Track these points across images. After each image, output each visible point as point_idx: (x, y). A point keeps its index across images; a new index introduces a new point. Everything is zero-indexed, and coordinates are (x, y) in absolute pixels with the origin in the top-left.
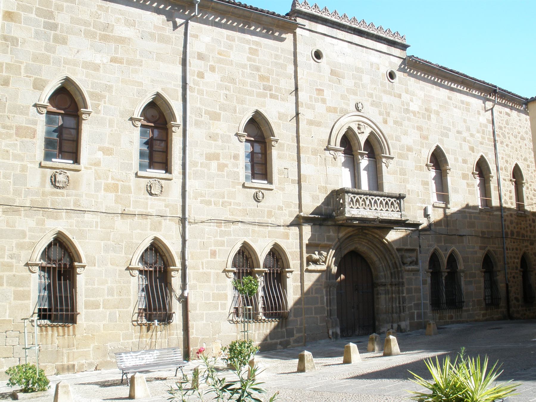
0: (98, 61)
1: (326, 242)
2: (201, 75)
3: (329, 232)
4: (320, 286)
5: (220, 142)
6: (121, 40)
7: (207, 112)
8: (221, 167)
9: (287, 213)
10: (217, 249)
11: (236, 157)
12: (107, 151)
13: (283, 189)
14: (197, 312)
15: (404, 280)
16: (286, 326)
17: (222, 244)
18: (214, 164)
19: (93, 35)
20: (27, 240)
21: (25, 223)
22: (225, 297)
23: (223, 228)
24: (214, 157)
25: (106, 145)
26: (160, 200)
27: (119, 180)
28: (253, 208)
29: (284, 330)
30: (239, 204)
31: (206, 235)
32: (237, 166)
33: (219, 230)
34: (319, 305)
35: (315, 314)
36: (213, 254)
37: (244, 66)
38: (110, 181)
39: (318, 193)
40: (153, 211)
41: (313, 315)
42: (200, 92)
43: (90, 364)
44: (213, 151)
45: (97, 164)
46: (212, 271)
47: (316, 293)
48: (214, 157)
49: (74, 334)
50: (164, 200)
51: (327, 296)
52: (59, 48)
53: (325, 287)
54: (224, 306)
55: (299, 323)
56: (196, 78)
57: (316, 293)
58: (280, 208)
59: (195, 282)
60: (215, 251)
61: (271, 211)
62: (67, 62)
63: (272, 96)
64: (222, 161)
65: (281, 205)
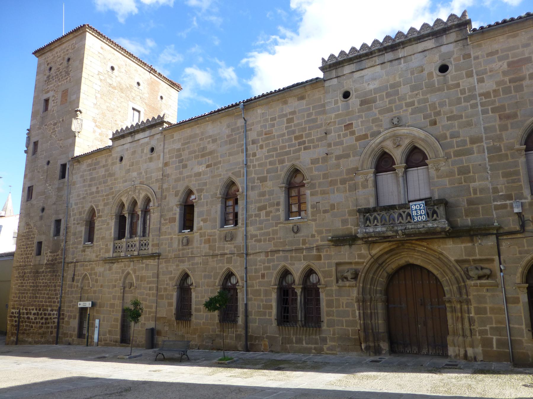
0: (201, 170)
1: (357, 260)
2: (254, 155)
3: (361, 251)
4: (350, 301)
5: (267, 197)
6: (211, 153)
7: (258, 179)
8: (268, 214)
9: (319, 238)
10: (266, 272)
11: (278, 204)
12: (205, 221)
13: (315, 220)
14: (253, 317)
15: (471, 297)
16: (319, 334)
17: (268, 268)
18: (263, 213)
19: (196, 157)
20: (172, 275)
21: (172, 267)
22: (271, 307)
23: (269, 257)
24: (260, 209)
25: (205, 217)
26: (231, 244)
27: (211, 236)
28: (291, 239)
29: (318, 337)
30: (280, 238)
31: (258, 264)
32: (278, 210)
33: (266, 258)
34: (351, 318)
35: (346, 326)
36: (263, 276)
37: (283, 135)
38: (207, 237)
39: (347, 217)
40: (227, 251)
41: (344, 327)
42: (254, 166)
43: (196, 345)
44: (262, 204)
45: (200, 229)
46: (262, 288)
47: (347, 307)
48: (260, 209)
49: (190, 327)
50: (234, 243)
51: (359, 309)
52: (184, 170)
53: (356, 302)
54: (270, 314)
55: (332, 333)
56: (251, 158)
57: (347, 307)
58: (313, 236)
59: (252, 296)
60: (264, 274)
61: (305, 239)
62: (188, 177)
63: (305, 149)
64: (268, 209)
65: (314, 233)
